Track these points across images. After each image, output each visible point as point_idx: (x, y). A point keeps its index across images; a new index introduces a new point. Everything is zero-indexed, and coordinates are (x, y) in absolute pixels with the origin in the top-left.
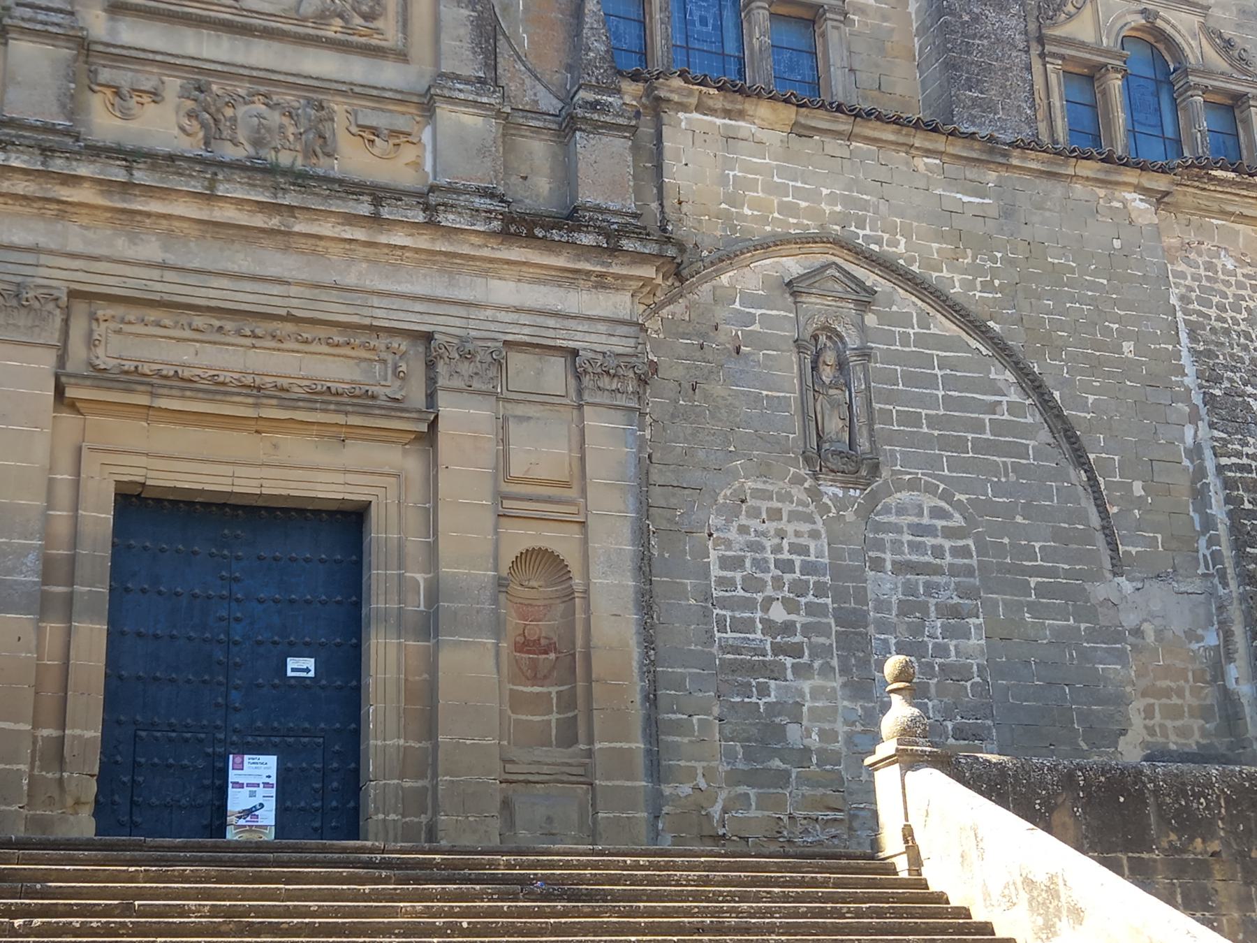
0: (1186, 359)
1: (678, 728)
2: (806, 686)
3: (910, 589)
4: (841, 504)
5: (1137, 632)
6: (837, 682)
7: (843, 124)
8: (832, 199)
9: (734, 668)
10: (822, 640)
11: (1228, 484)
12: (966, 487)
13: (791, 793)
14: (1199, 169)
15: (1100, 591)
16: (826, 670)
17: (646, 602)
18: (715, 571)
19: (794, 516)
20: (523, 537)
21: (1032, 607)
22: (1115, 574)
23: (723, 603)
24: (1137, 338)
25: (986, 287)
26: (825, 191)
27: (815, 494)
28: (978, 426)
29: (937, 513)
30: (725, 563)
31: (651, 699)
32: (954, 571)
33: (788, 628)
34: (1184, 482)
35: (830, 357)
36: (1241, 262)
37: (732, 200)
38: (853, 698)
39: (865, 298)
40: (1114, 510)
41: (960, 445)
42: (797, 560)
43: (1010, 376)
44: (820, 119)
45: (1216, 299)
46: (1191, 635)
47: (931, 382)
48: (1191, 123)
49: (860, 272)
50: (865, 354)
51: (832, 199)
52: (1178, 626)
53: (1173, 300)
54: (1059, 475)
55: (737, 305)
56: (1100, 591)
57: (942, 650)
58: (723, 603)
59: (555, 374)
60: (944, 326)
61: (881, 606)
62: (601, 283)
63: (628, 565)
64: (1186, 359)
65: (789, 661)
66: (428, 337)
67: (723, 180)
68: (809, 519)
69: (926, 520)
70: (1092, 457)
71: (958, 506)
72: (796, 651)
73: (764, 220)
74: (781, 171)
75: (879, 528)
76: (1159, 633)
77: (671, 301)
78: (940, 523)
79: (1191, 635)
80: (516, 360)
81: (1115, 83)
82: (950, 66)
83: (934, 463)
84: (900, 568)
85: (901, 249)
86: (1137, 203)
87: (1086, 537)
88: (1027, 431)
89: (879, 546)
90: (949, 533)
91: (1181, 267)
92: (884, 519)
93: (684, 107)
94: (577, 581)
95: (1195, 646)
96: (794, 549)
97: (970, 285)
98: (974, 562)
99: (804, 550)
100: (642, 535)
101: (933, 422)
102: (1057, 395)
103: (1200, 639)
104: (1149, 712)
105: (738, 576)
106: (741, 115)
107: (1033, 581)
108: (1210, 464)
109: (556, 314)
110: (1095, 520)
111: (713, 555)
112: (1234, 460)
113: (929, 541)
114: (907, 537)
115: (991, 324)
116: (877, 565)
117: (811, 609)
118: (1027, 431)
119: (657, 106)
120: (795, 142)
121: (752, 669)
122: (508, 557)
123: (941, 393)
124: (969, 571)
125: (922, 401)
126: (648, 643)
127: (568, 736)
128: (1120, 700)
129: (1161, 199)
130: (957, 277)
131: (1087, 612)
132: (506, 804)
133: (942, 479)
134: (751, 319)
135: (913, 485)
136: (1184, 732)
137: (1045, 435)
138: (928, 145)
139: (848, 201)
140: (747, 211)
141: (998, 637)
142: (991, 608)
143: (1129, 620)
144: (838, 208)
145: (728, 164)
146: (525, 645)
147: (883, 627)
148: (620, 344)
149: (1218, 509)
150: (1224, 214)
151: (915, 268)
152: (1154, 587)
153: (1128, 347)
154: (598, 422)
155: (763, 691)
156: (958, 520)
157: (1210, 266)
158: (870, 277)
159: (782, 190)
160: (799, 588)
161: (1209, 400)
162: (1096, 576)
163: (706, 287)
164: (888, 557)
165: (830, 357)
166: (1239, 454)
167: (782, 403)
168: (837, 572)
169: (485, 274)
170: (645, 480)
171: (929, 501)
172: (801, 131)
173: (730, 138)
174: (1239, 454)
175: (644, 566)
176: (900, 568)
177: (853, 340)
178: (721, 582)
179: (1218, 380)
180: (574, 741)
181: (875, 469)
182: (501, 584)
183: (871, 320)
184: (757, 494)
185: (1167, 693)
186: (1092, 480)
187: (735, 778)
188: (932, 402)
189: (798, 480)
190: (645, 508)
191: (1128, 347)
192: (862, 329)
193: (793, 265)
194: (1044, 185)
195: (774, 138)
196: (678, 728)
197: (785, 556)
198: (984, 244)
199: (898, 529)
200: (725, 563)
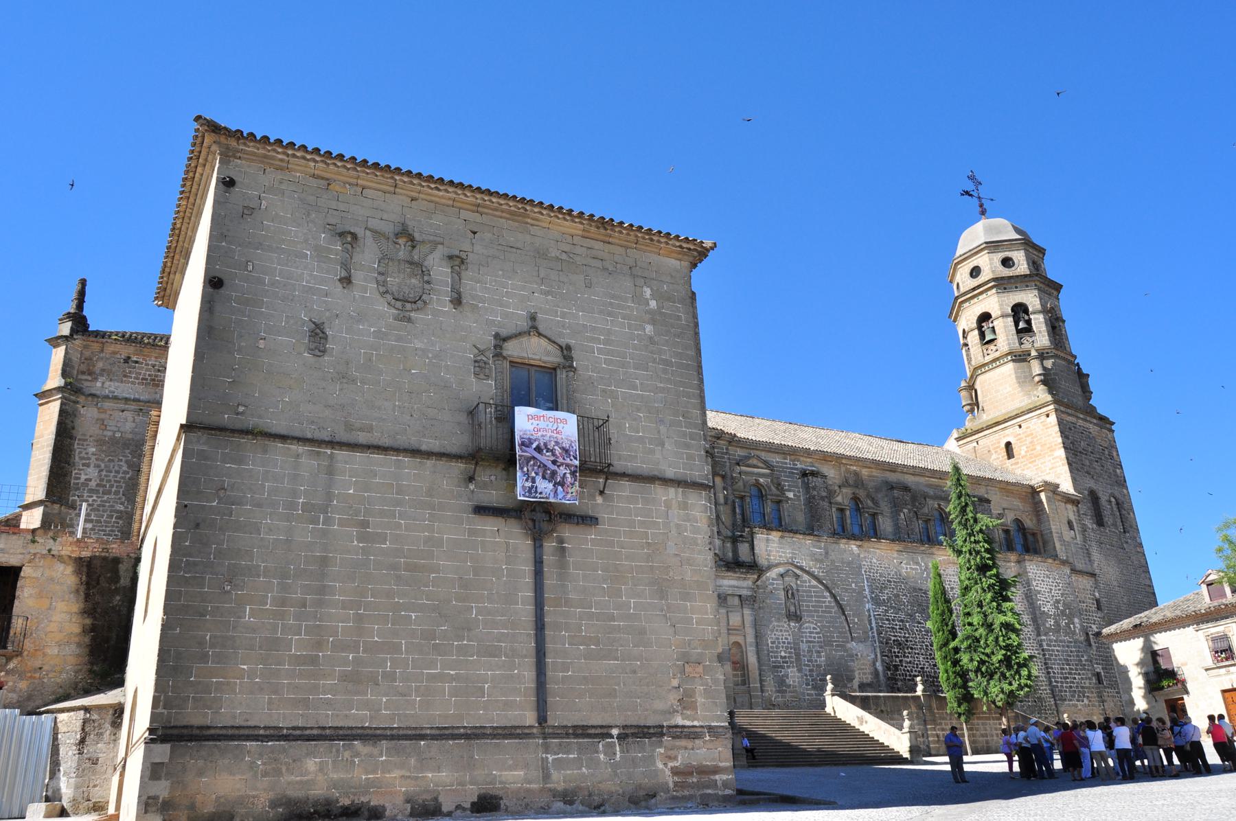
0: (866, 588)
1: (764, 681)
2: (789, 670)
3: (809, 647)
4: (795, 627)
5: (857, 655)
7: (792, 535)
8: (789, 553)
9: (775, 667)
11: (876, 619)
13: (788, 695)
14: (869, 538)
15: (849, 645)
16: (793, 667)
17: (758, 653)
18: (770, 645)
20: (733, 639)
23: (772, 652)
24: (856, 583)
25: (823, 572)
27: (789, 625)
28: (822, 607)
29: (814, 628)
30: (772, 643)
31: (760, 675)
32: (818, 642)
33: (785, 657)
34: (866, 618)
35: (790, 592)
36: (877, 560)
37: (769, 555)
39: (797, 577)
41: (818, 611)
43: (828, 594)
44: (787, 534)
46: (868, 656)
47: (811, 596)
48: (866, 521)
49: (796, 570)
50: (798, 591)
51: (789, 553)
52: (865, 654)
54: (839, 618)
56: (849, 645)
57: (816, 661)
58: (772, 652)
59: (736, 601)
60: (814, 583)
61: (804, 651)
62: (745, 579)
64: (866, 588)
67: (767, 550)
68: (788, 631)
71: (819, 627)
72: (787, 662)
75: (803, 633)
77: (757, 580)
80: (729, 598)
81: (848, 513)
82: (812, 516)
83: (813, 616)
86: (854, 548)
87: (845, 633)
88: (833, 607)
90: (817, 633)
91: (864, 563)
94: (744, 650)
96: (787, 639)
97: (819, 572)
100: (756, 637)
101: (813, 606)
104: (859, 674)
108: (872, 614)
109: (737, 587)
110: (847, 629)
116: (802, 641)
117: (790, 653)
118: (833, 607)
119: (752, 534)
120: (781, 540)
121: (778, 667)
122: (731, 643)
124: (821, 642)
125: (809, 601)
126: (759, 662)
127: (744, 683)
128: (853, 671)
131: (846, 651)
132: (734, 698)
134: (774, 584)
135: (809, 622)
137: (836, 608)
139: (793, 553)
141: (828, 657)
142: (826, 652)
143: (854, 652)
146: (734, 663)
148: (749, 593)
149: (874, 625)
150: (873, 548)
152: (860, 644)
153: (853, 585)
154: (747, 612)
155: (781, 672)
156: (818, 630)
157: (871, 562)
159: (778, 552)
161: (872, 598)
162: (848, 642)
163: (764, 577)
165: (790, 592)
167: (781, 604)
168: (794, 643)
169: (723, 579)
170: (755, 625)
171: (812, 626)
172: (782, 537)
173: (768, 540)
175: (757, 645)
177: (794, 587)
178: (772, 647)
179: (873, 593)
180: (745, 684)
181: (801, 619)
182: (730, 649)
183: (799, 582)
184: (778, 626)
185: (862, 669)
186: (847, 619)
187: (778, 691)
188: (811, 601)
189: (785, 622)
190: (756, 629)
191: (853, 585)
192: (797, 584)
193: (781, 570)
194: (835, 545)
195: (776, 539)
196: (764, 681)
198: (821, 561)
199: (806, 632)
200: (772, 643)
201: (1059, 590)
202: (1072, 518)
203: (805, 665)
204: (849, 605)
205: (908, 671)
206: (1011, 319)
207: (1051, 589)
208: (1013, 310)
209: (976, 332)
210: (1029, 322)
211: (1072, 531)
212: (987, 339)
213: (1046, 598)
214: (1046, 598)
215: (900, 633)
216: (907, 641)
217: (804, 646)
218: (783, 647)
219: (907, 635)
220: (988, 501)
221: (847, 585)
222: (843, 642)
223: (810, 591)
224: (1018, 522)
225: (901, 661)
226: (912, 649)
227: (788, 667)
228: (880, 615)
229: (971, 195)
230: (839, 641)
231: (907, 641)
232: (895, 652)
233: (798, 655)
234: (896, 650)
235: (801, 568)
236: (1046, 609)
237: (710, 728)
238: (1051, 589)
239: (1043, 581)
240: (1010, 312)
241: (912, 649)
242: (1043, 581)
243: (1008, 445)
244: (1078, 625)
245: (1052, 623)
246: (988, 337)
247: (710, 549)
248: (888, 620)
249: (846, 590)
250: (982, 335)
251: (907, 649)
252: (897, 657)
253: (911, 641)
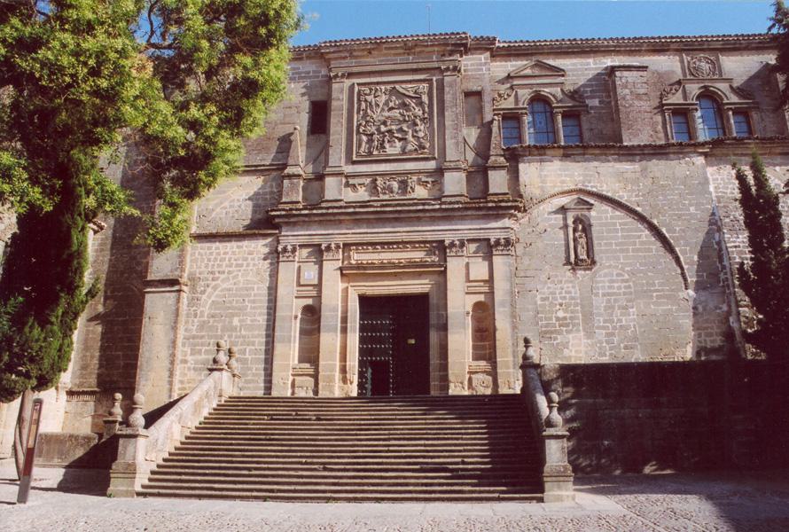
2: (570, 336)
3: (609, 301)
6: (582, 333)
10: (577, 321)
12: (630, 265)
16: (578, 331)
18: (539, 302)
19: (566, 282)
21: (653, 303)
22: (686, 289)
26: (576, 174)
29: (618, 275)
30: (543, 299)
32: (625, 294)
33: (565, 318)
37: (543, 182)
38: (588, 338)
42: (568, 296)
46: (716, 308)
47: (617, 231)
63: (508, 305)
69: (614, 278)
72: (567, 325)
73: (555, 186)
74: (560, 170)
75: (597, 282)
76: (704, 309)
78: (620, 278)
79: (716, 308)
84: (604, 295)
89: (598, 288)
90: (623, 281)
92: (599, 279)
93: (526, 156)
95: (718, 311)
98: (632, 290)
99: (570, 292)
103: (720, 308)
105: (547, 303)
106: (545, 154)
107: (655, 294)
111: (539, 297)
112: (733, 244)
113: (616, 285)
114: (607, 284)
115: (639, 209)
116: (597, 295)
121: (552, 332)
123: (620, 234)
124: (631, 293)
129: (706, 155)
130: (625, 194)
133: (622, 263)
135: (609, 267)
136: (712, 341)
138: (612, 152)
144: (581, 178)
145: (541, 170)
147: (599, 315)
156: (626, 277)
160: (568, 305)
164: (600, 291)
166: (734, 242)
174: (734, 242)
176: (604, 295)
185: (706, 328)
197: (564, 295)
199: (604, 282)
200: (543, 299)
203: (599, 328)
204: (683, 238)
217: (599, 303)
218: (561, 305)
221: (678, 209)
222: (672, 290)
223: (615, 224)
227: (568, 332)
228: (739, 247)
230: (663, 290)
233: (588, 317)
249: (679, 217)
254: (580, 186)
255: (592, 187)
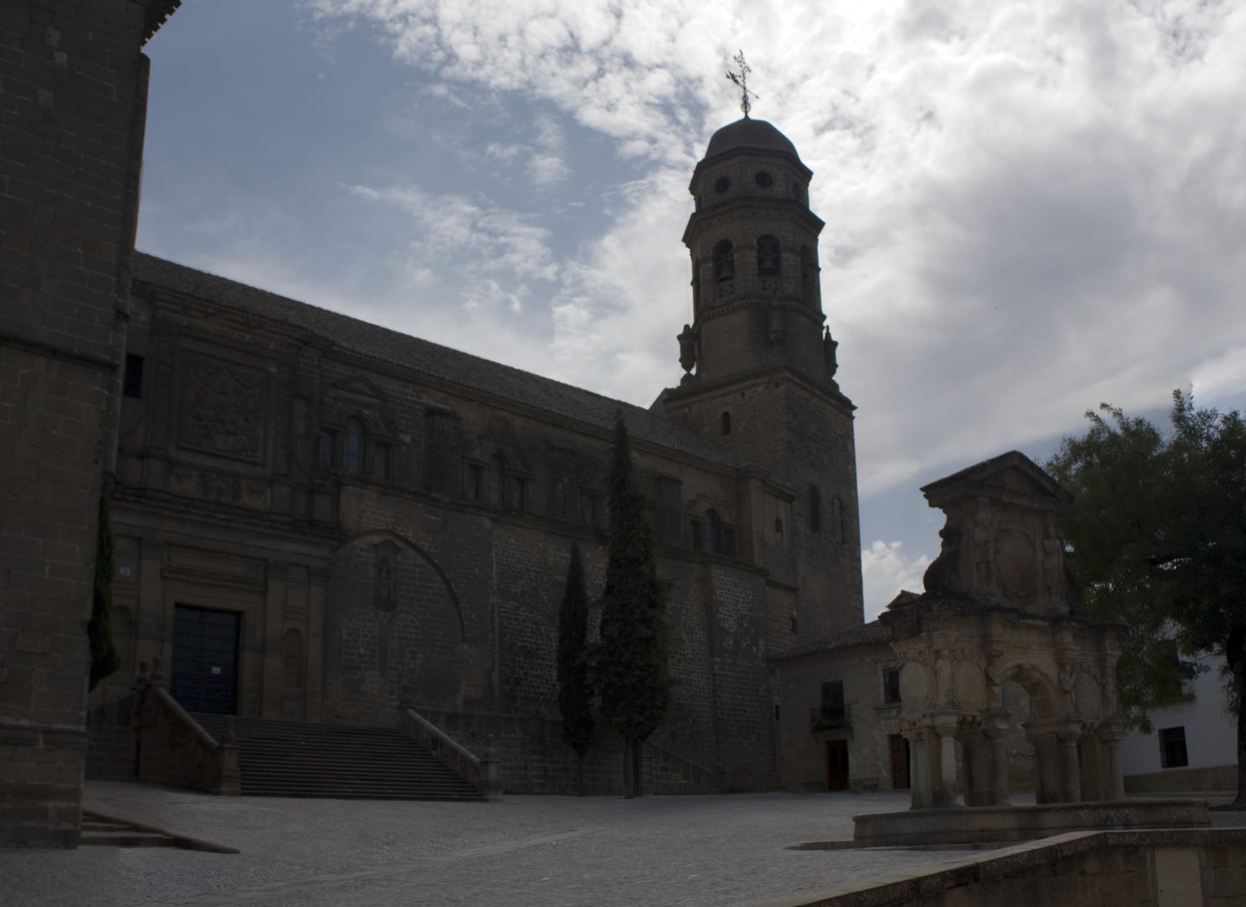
18: (344, 637)
40: (465, 622)
45: (506, 554)
53: (493, 555)
55: (358, 551)
60: (421, 561)
64: (494, 575)
65: (363, 665)
66: (266, 560)
70: (461, 605)
85: (410, 535)
86: (486, 522)
102: (453, 585)
107: (438, 644)
115: (436, 561)
129: (493, 520)
140: (364, 520)
151: (414, 541)
153: (477, 570)
158: (399, 544)
183: (399, 558)
193: (377, 539)
201: (748, 603)
202: (782, 517)
205: (533, 687)
206: (754, 254)
207: (738, 602)
208: (759, 243)
209: (710, 265)
210: (777, 262)
211: (779, 535)
212: (723, 275)
213: (729, 611)
214: (729, 611)
215: (531, 637)
216: (538, 649)
219: (540, 642)
220: (679, 483)
224: (712, 512)
225: (526, 674)
226: (543, 659)
228: (507, 612)
229: (736, 81)
231: (538, 649)
232: (519, 662)
234: (522, 660)
235: (405, 540)
236: (726, 626)
237: (48, 732)
238: (738, 602)
239: (729, 590)
240: (755, 244)
241: (543, 659)
242: (729, 590)
243: (726, 416)
244: (762, 648)
245: (731, 643)
246: (725, 274)
247: (96, 462)
248: (515, 619)
250: (718, 269)
251: (537, 659)
252: (522, 668)
253: (544, 649)
254: (391, 527)
255: (401, 531)
